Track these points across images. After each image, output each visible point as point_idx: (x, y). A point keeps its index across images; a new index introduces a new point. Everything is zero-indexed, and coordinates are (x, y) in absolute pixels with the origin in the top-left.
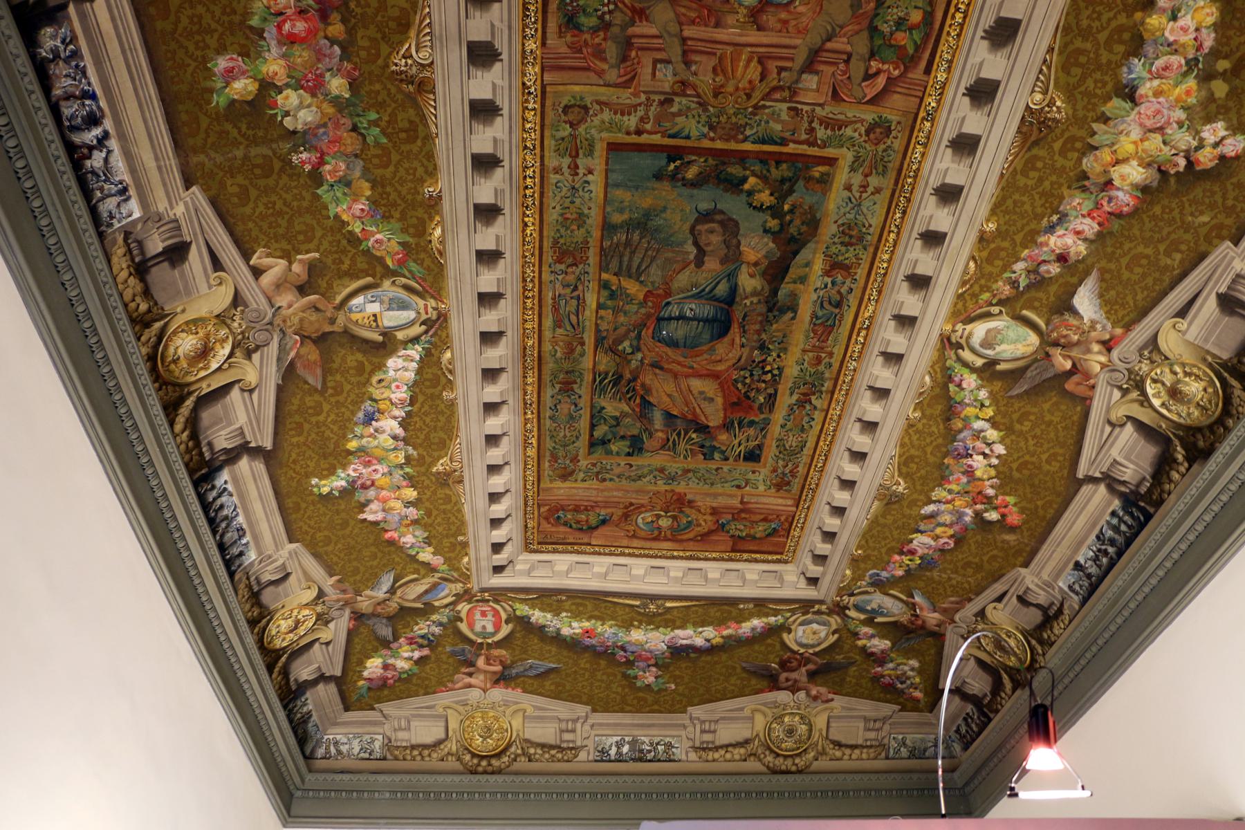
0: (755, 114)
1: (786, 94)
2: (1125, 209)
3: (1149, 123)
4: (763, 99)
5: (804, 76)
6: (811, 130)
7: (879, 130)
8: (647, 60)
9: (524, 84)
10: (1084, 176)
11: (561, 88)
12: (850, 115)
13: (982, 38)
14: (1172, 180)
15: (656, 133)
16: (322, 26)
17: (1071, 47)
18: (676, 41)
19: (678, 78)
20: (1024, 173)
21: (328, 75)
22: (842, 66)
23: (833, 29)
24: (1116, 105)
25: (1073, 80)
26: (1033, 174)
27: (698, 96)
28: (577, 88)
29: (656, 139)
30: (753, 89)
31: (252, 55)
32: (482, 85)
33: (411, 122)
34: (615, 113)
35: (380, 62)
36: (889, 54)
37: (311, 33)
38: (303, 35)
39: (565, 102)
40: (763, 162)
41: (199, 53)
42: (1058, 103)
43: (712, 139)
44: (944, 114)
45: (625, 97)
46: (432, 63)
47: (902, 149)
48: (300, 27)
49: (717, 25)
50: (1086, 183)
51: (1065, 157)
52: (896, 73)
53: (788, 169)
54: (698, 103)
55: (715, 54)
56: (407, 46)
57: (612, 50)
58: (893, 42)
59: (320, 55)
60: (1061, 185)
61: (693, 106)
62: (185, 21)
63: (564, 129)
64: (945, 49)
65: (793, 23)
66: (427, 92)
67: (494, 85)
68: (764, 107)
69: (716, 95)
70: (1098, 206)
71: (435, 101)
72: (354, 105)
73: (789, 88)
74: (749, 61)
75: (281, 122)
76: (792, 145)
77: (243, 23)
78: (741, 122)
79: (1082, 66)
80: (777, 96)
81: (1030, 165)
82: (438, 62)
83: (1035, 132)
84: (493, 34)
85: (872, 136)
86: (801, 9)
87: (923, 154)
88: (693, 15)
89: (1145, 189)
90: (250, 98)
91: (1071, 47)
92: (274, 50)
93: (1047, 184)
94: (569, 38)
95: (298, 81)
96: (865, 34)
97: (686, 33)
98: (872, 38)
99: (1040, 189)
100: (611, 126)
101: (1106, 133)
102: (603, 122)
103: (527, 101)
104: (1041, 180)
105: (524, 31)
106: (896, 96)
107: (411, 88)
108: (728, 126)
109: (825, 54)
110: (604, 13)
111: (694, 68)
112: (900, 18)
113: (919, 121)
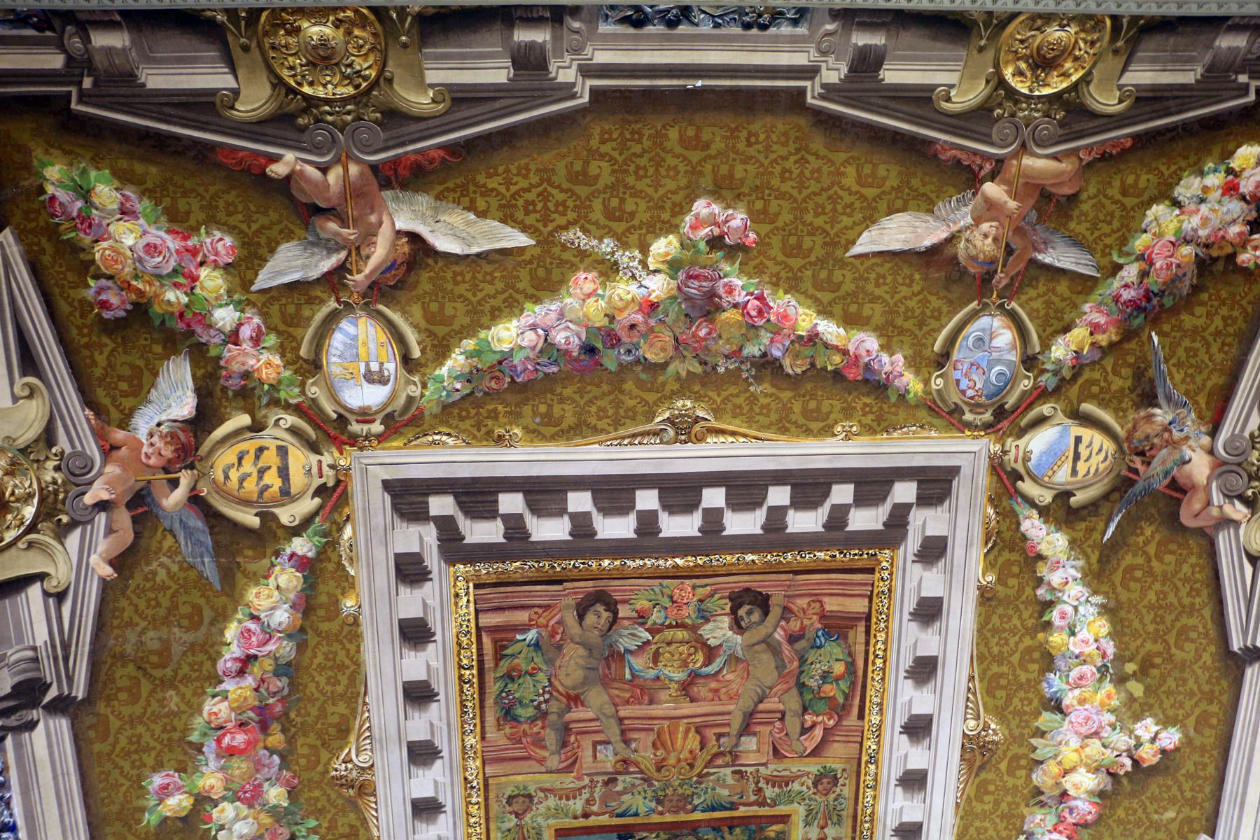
0: (701, 783)
1: (728, 758)
2: (1089, 817)
3: (1083, 730)
4: (706, 767)
5: (743, 739)
6: (759, 791)
7: (826, 780)
8: (587, 742)
9: (466, 779)
10: (1038, 792)
11: (503, 779)
12: (794, 770)
13: (905, 678)
14: (1125, 781)
15: (603, 814)
16: (262, 737)
17: (990, 673)
18: (613, 722)
19: (619, 757)
20: (979, 799)
21: (266, 785)
22: (778, 724)
23: (763, 691)
24: (1046, 719)
25: (1001, 703)
26: (987, 798)
27: (641, 772)
28: (519, 778)
29: (605, 820)
30: (694, 758)
31: (189, 770)
32: (424, 783)
33: (351, 826)
34: (561, 799)
35: (320, 768)
36: (821, 706)
37: (250, 744)
38: (243, 747)
39: (508, 792)
40: (716, 829)
41: (135, 772)
42: (993, 726)
43: (661, 813)
44: (887, 755)
45: (569, 781)
46: (372, 765)
47: (853, 796)
48: (240, 739)
49: (651, 702)
50: (1042, 798)
51: (1014, 776)
52: (832, 723)
53: (742, 832)
54: (642, 779)
55: (652, 730)
56: (346, 751)
57: (551, 738)
58: (822, 695)
59: (259, 766)
60: (1018, 805)
61: (638, 782)
62: (123, 741)
63: (510, 820)
64: (873, 693)
65: (724, 690)
66: (367, 794)
67: (436, 782)
68: (709, 774)
69: (659, 769)
70: (1061, 820)
71: (376, 803)
72: (293, 814)
73: (730, 752)
74: (687, 731)
75: (215, 836)
76: (742, 808)
77: (182, 739)
78: (688, 792)
79: (1004, 688)
80: (720, 761)
81: (982, 790)
82: (378, 765)
83: (979, 757)
84: (432, 733)
85: (820, 787)
86: (730, 677)
87: (875, 797)
88: (627, 695)
89: (1102, 794)
90: (183, 814)
91: (990, 673)
92: (213, 764)
93: (1004, 806)
94: (508, 730)
95: (235, 793)
96: (795, 691)
97: (622, 713)
98: (801, 694)
99: (999, 812)
100: (558, 812)
101: (1046, 746)
102: (549, 809)
103: (470, 796)
104: (997, 803)
105: (462, 727)
106: (836, 745)
107: (351, 792)
108: (675, 798)
109: (759, 715)
110: (540, 703)
111: (633, 745)
113: (863, 766)
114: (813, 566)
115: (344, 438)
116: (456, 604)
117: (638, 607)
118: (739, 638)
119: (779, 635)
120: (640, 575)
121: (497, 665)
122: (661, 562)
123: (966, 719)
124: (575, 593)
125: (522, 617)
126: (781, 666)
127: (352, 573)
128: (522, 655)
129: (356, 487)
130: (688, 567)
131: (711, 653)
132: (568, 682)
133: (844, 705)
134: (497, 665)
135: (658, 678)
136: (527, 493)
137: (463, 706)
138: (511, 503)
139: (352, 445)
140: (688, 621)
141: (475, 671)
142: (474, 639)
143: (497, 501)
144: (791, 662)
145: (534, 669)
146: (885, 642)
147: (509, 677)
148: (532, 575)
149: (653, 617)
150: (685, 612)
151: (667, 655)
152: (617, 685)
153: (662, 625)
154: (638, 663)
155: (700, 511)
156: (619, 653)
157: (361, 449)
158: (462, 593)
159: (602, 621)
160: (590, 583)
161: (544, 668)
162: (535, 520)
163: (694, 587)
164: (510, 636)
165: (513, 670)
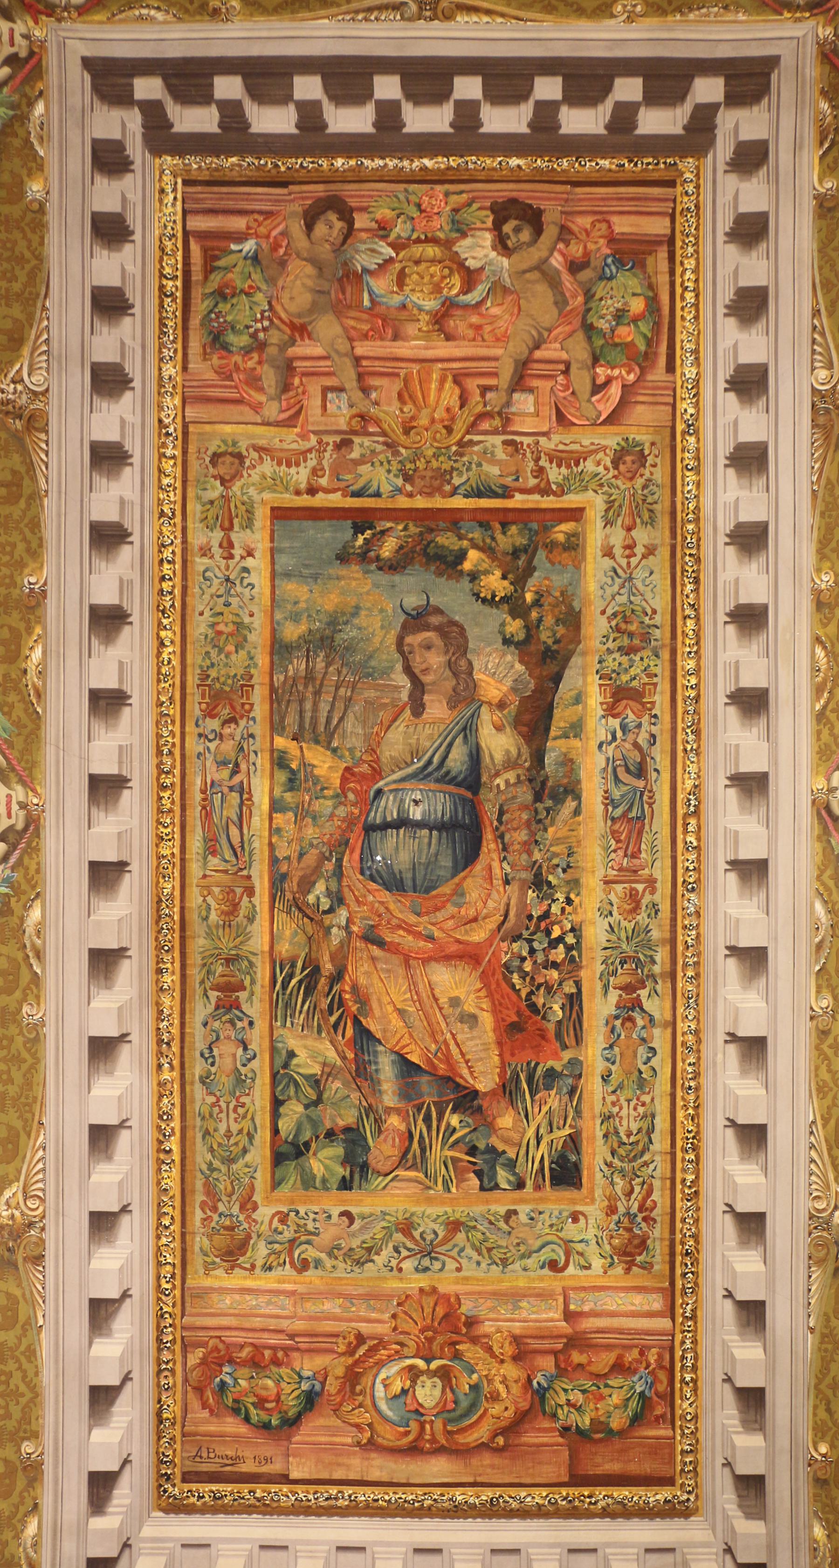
1: (497, 422)
5: (516, 396)
8: (314, 388)
22: (561, 379)
23: (540, 334)
49: (396, 337)
52: (632, 377)
57: (269, 377)
58: (617, 340)
64: (684, 336)
65: (488, 328)
69: (407, 431)
73: (500, 414)
74: (442, 381)
86: (495, 311)
88: (365, 327)
96: (580, 336)
97: (359, 351)
98: (589, 338)
105: (160, 352)
106: (640, 408)
111: (374, 395)
112: (618, 310)
114: (595, 177)
115: (41, 7)
116: (161, 201)
117: (378, 216)
118: (505, 262)
119: (557, 261)
120: (380, 177)
121: (206, 278)
122: (406, 163)
123: (813, 369)
124: (303, 198)
125: (239, 223)
126: (561, 302)
127: (42, 153)
128: (237, 269)
129: (51, 61)
130: (439, 169)
131: (470, 278)
132: (293, 308)
133: (646, 353)
134: (206, 278)
135: (404, 307)
136: (245, 77)
137: (162, 324)
138: (228, 87)
139: (49, 15)
140: (441, 235)
141: (179, 283)
142: (180, 245)
143: (212, 85)
144: (575, 297)
145: (251, 287)
146: (696, 271)
147: (221, 294)
148: (252, 174)
149: (397, 230)
150: (436, 223)
151: (415, 277)
152: (353, 314)
153: (409, 239)
154: (380, 285)
155: (452, 102)
156: (355, 273)
157: (59, 20)
158: (169, 189)
159: (335, 232)
160: (321, 187)
161: (264, 287)
162: (255, 107)
163: (447, 194)
164: (222, 244)
165: (227, 286)
